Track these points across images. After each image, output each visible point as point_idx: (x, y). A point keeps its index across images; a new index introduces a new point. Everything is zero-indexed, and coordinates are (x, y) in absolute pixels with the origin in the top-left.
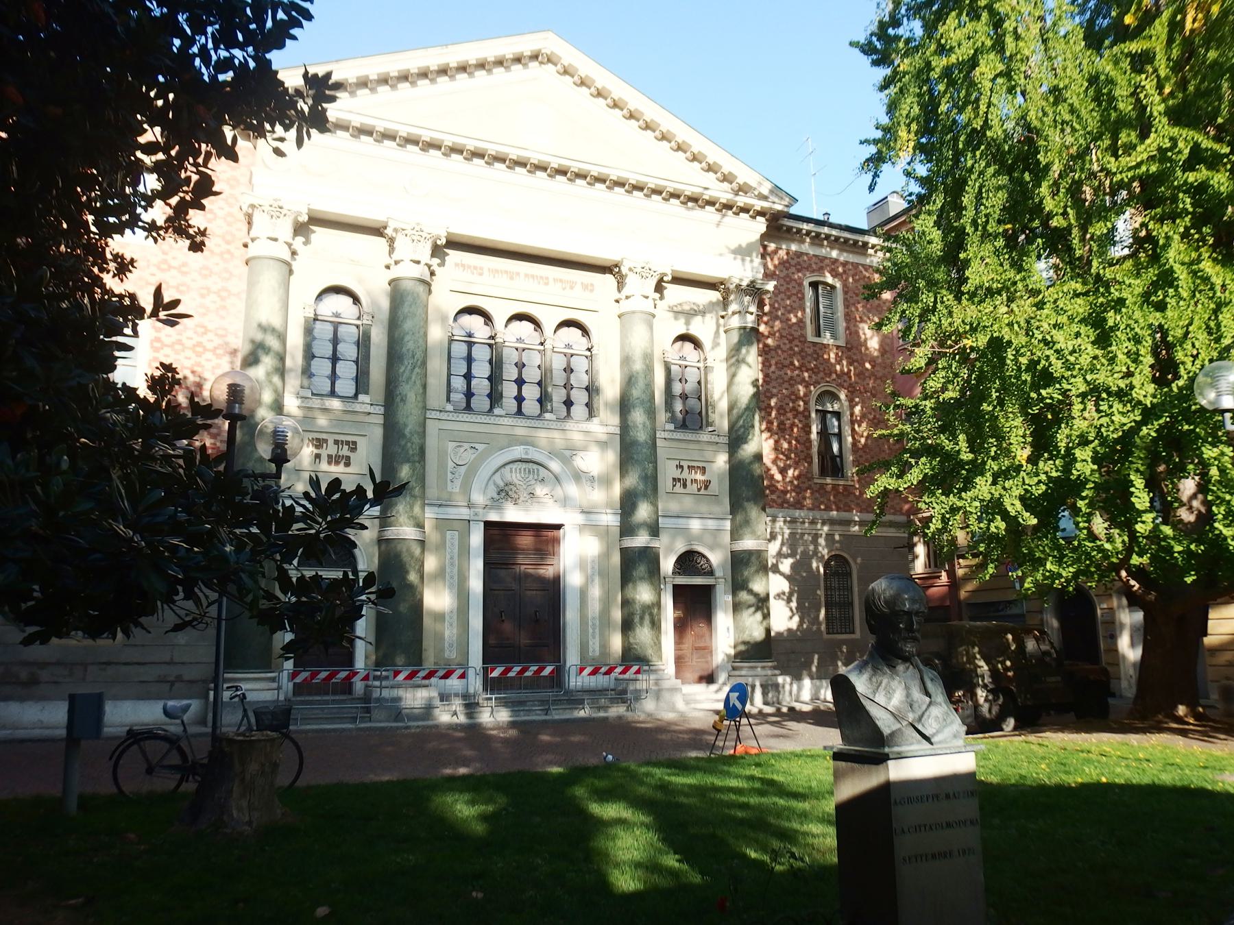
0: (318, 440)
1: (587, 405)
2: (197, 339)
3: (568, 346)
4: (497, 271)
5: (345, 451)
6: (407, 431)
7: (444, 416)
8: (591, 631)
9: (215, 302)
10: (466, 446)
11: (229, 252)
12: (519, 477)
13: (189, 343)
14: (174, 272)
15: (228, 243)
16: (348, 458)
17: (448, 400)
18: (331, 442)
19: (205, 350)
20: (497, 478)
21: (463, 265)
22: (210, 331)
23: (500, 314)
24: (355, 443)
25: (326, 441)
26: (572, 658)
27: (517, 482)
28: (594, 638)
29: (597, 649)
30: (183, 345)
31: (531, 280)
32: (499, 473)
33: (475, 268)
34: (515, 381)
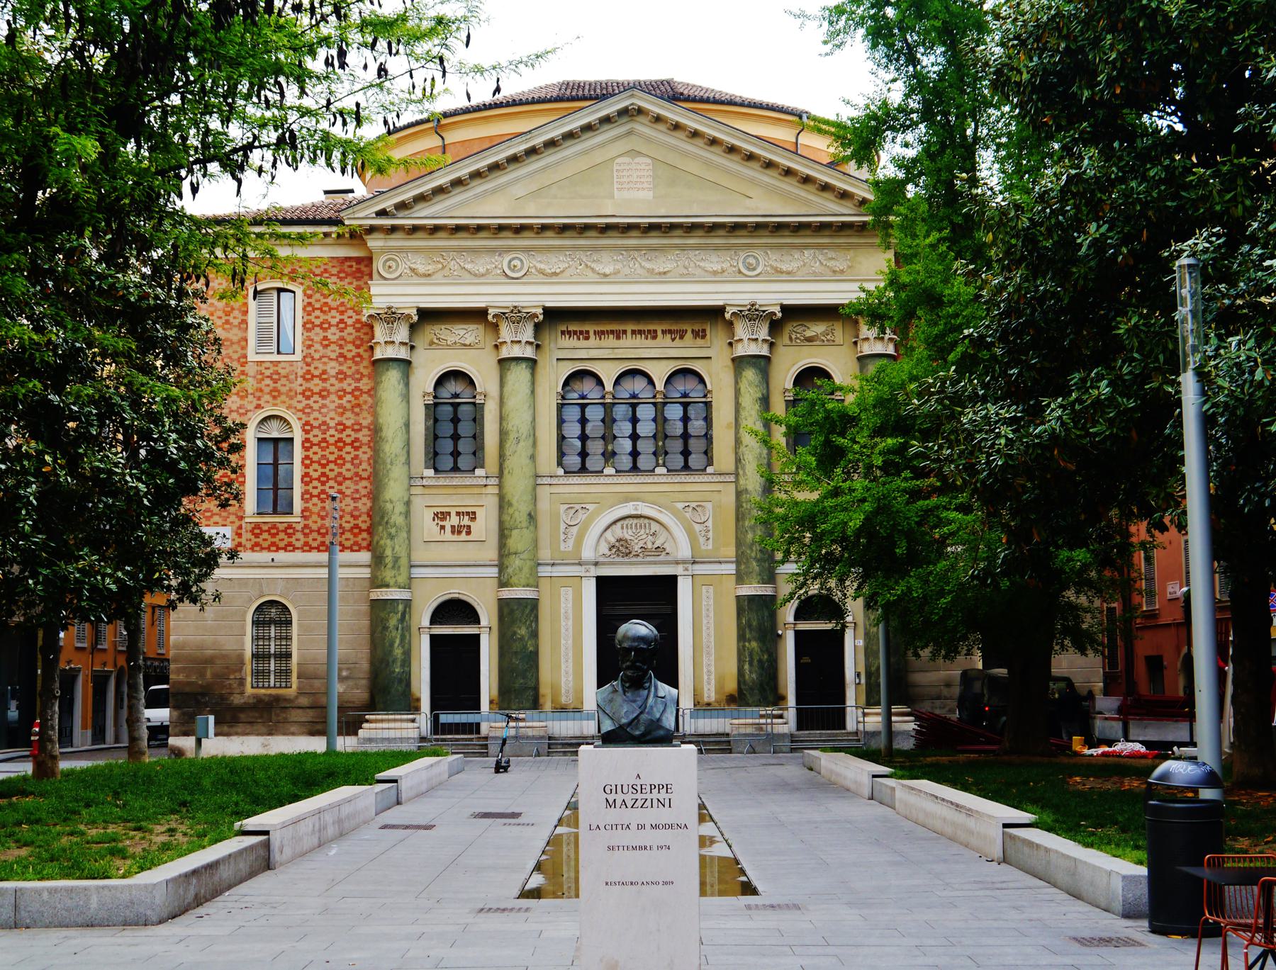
1: (706, 453)
2: (337, 436)
3: (685, 395)
4: (603, 332)
5: (466, 521)
7: (554, 481)
8: (705, 677)
9: (350, 402)
10: (577, 507)
11: (359, 355)
12: (630, 533)
13: (332, 440)
14: (316, 381)
15: (358, 347)
16: (469, 527)
17: (560, 464)
18: (453, 514)
19: (346, 444)
20: (608, 534)
21: (569, 332)
22: (348, 427)
23: (608, 374)
24: (474, 513)
25: (449, 514)
27: (628, 538)
28: (709, 684)
29: (713, 695)
30: (327, 442)
31: (639, 336)
32: (610, 530)
33: (581, 332)
34: (630, 437)
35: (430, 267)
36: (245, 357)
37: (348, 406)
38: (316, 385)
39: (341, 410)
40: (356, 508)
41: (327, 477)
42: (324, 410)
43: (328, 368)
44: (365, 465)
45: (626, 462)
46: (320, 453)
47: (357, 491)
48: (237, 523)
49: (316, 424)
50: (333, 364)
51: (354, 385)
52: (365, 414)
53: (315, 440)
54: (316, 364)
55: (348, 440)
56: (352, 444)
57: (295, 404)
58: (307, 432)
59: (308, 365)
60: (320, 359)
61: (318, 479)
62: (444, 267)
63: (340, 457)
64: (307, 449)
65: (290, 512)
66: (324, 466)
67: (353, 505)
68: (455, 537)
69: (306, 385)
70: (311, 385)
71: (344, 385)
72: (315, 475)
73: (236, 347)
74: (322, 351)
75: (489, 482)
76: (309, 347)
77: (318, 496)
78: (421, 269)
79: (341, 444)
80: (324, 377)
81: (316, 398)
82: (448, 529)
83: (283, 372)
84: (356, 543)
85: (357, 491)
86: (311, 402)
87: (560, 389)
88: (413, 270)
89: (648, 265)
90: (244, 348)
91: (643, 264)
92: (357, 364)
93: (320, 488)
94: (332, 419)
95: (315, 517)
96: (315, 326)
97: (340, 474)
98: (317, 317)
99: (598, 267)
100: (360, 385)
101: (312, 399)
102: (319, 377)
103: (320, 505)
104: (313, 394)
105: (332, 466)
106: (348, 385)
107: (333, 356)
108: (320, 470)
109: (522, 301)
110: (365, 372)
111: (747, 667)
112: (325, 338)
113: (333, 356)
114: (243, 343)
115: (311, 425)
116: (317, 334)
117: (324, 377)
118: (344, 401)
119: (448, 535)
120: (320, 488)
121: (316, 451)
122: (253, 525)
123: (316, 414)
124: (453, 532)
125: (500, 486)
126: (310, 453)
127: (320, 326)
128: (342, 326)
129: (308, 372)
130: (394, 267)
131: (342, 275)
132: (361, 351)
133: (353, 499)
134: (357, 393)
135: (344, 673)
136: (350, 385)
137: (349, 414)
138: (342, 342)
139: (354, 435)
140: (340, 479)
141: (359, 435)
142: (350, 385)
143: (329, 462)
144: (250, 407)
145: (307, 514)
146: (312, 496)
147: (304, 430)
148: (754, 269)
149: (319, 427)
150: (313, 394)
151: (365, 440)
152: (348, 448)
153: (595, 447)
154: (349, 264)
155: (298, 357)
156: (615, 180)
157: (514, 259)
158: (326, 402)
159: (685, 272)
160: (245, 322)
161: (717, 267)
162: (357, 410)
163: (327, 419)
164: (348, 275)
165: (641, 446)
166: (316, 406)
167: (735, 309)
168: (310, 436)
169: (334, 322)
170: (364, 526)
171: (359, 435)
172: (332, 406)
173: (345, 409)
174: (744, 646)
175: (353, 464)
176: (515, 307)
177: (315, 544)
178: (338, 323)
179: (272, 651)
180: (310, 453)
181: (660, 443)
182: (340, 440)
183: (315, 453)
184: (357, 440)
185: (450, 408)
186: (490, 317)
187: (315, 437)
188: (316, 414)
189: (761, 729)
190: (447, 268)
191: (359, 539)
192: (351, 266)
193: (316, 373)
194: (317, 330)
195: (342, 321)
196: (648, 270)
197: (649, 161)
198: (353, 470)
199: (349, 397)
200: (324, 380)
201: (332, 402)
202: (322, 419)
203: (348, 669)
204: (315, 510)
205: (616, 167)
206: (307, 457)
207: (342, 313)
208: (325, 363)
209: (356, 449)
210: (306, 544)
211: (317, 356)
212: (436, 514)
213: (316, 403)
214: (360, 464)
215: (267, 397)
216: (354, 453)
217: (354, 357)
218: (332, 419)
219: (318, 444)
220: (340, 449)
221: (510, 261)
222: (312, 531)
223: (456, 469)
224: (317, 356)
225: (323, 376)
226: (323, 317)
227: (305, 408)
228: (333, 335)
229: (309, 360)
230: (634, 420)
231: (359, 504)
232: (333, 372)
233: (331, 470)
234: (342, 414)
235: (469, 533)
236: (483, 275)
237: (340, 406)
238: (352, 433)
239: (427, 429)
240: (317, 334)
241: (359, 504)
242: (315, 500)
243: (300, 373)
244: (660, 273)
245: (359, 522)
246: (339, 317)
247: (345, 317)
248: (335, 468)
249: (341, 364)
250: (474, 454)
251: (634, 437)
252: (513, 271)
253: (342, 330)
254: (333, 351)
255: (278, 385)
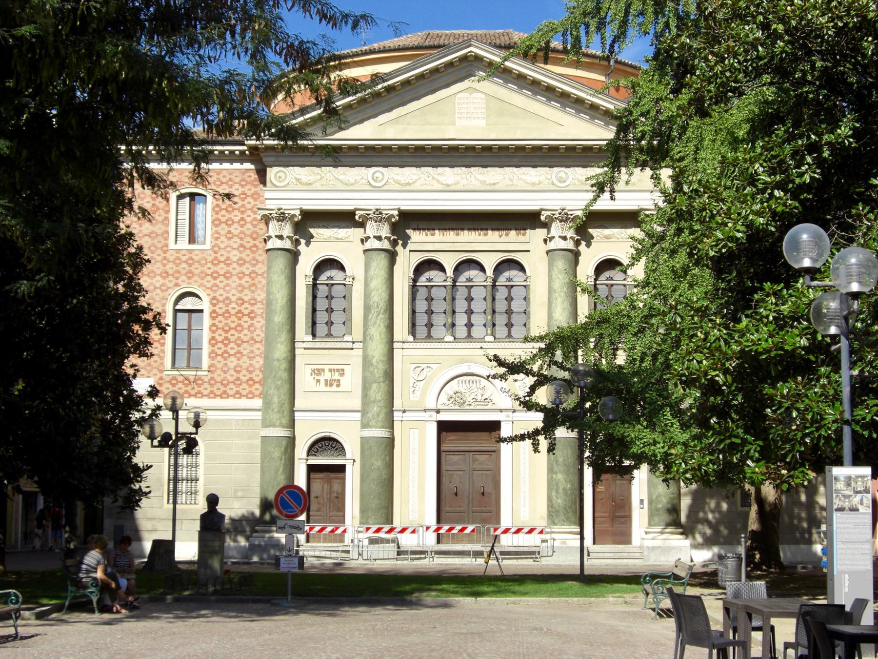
0: (318, 370)
2: (238, 308)
5: (336, 376)
6: (374, 361)
7: (406, 345)
11: (255, 246)
13: (233, 312)
14: (222, 265)
15: (254, 239)
16: (339, 381)
18: (327, 371)
19: (244, 315)
23: (449, 262)
24: (343, 370)
25: (323, 370)
26: (506, 521)
27: (463, 391)
35: (311, 178)
36: (167, 246)
37: (246, 285)
38: (221, 269)
39: (240, 288)
40: (251, 365)
41: (229, 340)
42: (228, 288)
43: (231, 255)
44: (258, 332)
45: (461, 331)
46: (224, 321)
47: (252, 352)
48: (159, 375)
49: (221, 299)
50: (235, 252)
51: (251, 269)
52: (259, 291)
53: (220, 312)
54: (222, 252)
55: (246, 312)
56: (248, 315)
57: (206, 283)
58: (214, 305)
59: (216, 253)
60: (225, 248)
61: (222, 342)
62: (322, 178)
63: (239, 325)
64: (214, 318)
65: (198, 368)
66: (227, 332)
67: (248, 362)
68: (328, 389)
69: (214, 268)
70: (217, 268)
71: (243, 269)
72: (220, 339)
73: (160, 238)
74: (227, 242)
75: (354, 346)
76: (217, 239)
77: (222, 355)
78: (304, 179)
79: (240, 315)
80: (228, 262)
81: (221, 278)
82: (323, 382)
83: (196, 258)
84: (251, 392)
85: (252, 352)
86: (217, 282)
87: (411, 275)
88: (298, 180)
89: (481, 178)
90: (166, 239)
91: (477, 176)
92: (253, 252)
93: (224, 348)
94: (234, 295)
95: (219, 372)
96: (221, 222)
97: (239, 338)
98: (223, 216)
99: (441, 178)
100: (256, 269)
101: (219, 280)
102: (224, 262)
103: (223, 362)
104: (219, 275)
105: (233, 332)
106: (247, 269)
107: (235, 246)
108: (224, 335)
109: (383, 205)
110: (260, 259)
111: (554, 493)
112: (229, 232)
113: (235, 246)
114: (165, 235)
115: (217, 300)
116: (223, 229)
117: (228, 262)
118: (243, 282)
119: (322, 387)
120: (224, 348)
121: (221, 322)
122: (171, 377)
123: (221, 292)
124: (326, 385)
125: (365, 349)
126: (216, 322)
127: (226, 223)
128: (242, 222)
129: (216, 258)
130: (283, 177)
131: (243, 183)
132: (257, 242)
133: (249, 357)
134: (253, 275)
135: (240, 494)
136: (248, 269)
137: (247, 291)
138: (242, 236)
139: (250, 308)
140: (239, 342)
141: (255, 308)
142: (248, 269)
143: (231, 328)
144: (171, 285)
145: (212, 369)
146: (217, 355)
147: (212, 304)
148: (564, 182)
149: (223, 301)
150: (219, 275)
151: (259, 312)
152: (246, 318)
153: (439, 320)
154: (248, 174)
155: (208, 246)
156: (457, 111)
157: (376, 172)
158: (229, 282)
159: (510, 183)
160: (167, 219)
161: (536, 180)
162: (253, 288)
163: (230, 295)
164: (247, 183)
165: (475, 319)
166: (221, 285)
167: (549, 213)
168: (216, 308)
169: (236, 219)
170: (257, 379)
171: (255, 308)
172: (234, 285)
173: (244, 288)
174: (552, 478)
175: (249, 330)
176: (377, 210)
177: (218, 393)
178: (240, 220)
179: (184, 476)
180: (216, 322)
181: (489, 317)
182: (240, 312)
183: (220, 322)
184: (252, 312)
185: (326, 288)
186: (357, 217)
187: (221, 308)
188: (221, 292)
189: (564, 543)
190: (324, 179)
191: (253, 389)
192: (250, 176)
193: (222, 259)
194: (223, 225)
195: (242, 219)
196: (481, 182)
197: (483, 96)
198: (249, 335)
199: (247, 278)
200: (228, 265)
201: (234, 282)
202: (225, 295)
203: (242, 490)
204: (219, 365)
205: (457, 101)
206: (214, 325)
207: (243, 212)
208: (229, 252)
209: (252, 319)
210: (212, 392)
211: (222, 246)
212: (313, 371)
213: (221, 282)
214: (255, 330)
215: (184, 278)
216: (250, 322)
217: (251, 247)
218: (233, 295)
219: (222, 315)
220: (239, 319)
221: (374, 174)
222: (216, 382)
223: (330, 335)
224: (222, 246)
225: (227, 262)
226: (228, 216)
227: (212, 286)
228: (235, 229)
229: (216, 249)
230: (470, 299)
231: (254, 362)
232: (235, 259)
233: (233, 335)
234: (241, 291)
235: (338, 386)
236: (352, 184)
237: (240, 285)
238: (249, 306)
239: (307, 304)
240: (223, 229)
241: (254, 362)
242: (219, 358)
243: (209, 259)
244: (490, 184)
245: (253, 376)
246: (240, 216)
247: (244, 216)
248: (236, 333)
249: (241, 252)
250: (344, 323)
251: (470, 312)
252: (375, 181)
253: (242, 226)
254: (235, 242)
255: (192, 268)
